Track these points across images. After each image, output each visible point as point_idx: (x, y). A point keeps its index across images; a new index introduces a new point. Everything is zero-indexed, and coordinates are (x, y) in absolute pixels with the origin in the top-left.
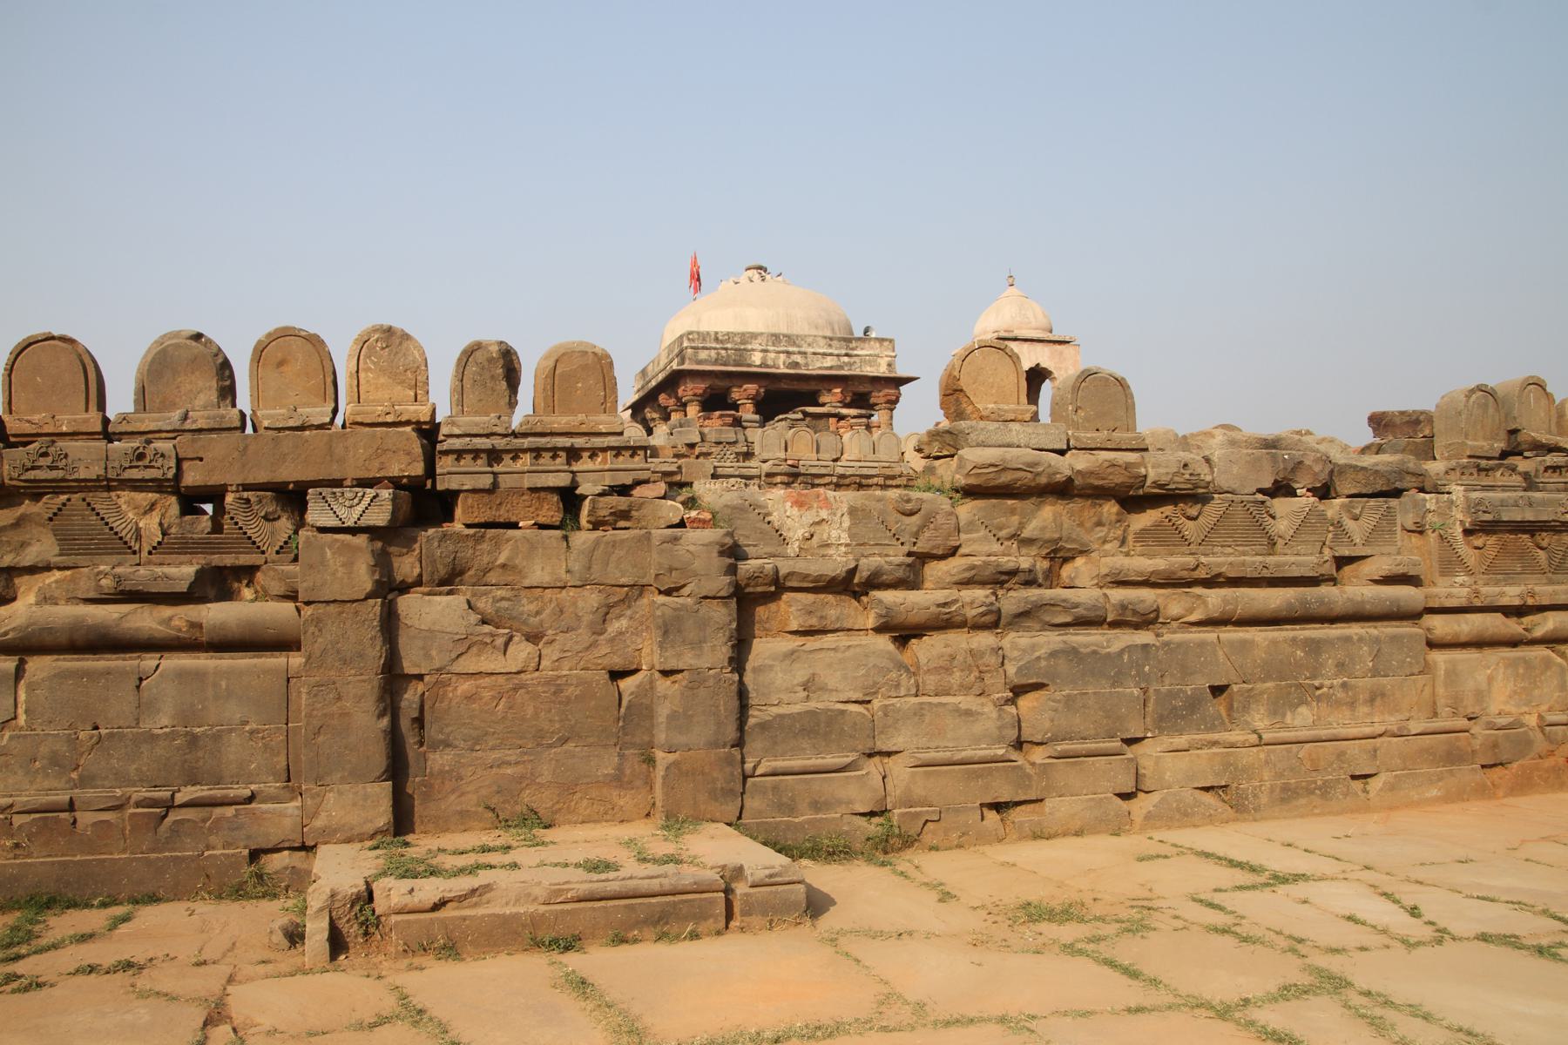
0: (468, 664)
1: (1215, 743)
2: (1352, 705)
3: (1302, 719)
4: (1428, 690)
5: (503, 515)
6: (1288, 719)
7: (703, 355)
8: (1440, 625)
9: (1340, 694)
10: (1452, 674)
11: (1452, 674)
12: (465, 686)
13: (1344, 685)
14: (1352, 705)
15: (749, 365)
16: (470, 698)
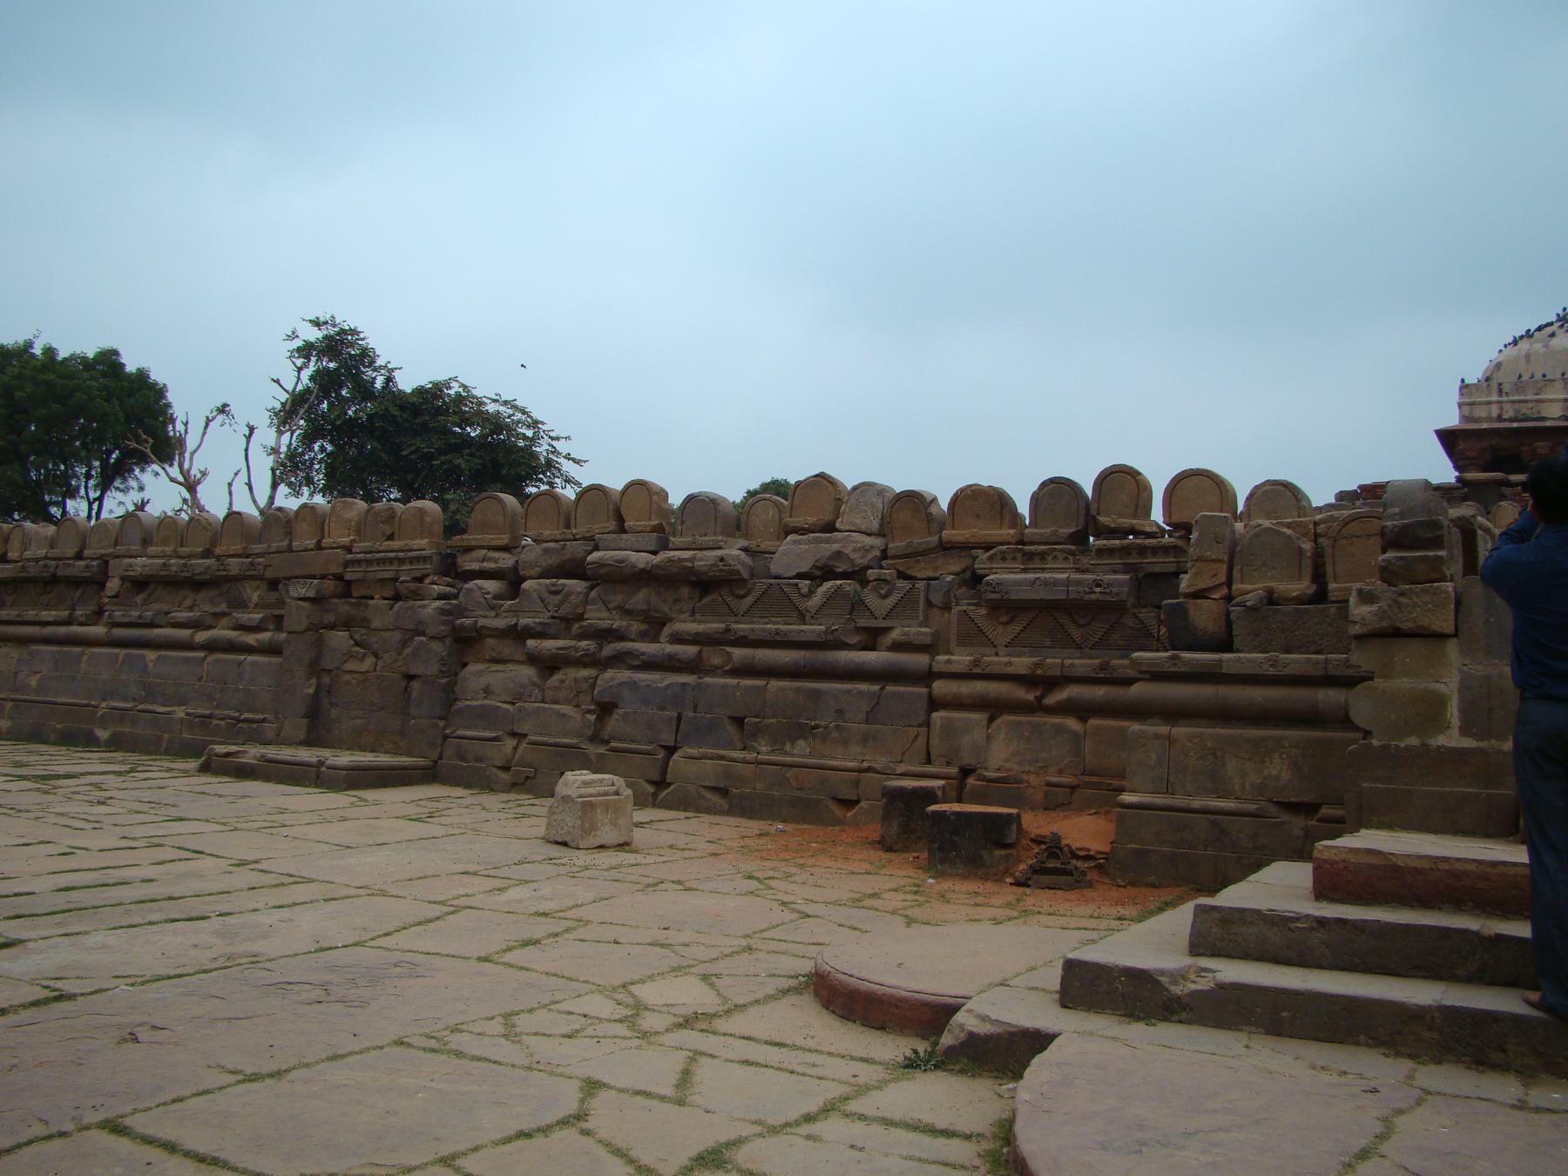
0: (350, 666)
1: (722, 758)
2: (846, 743)
3: (800, 750)
4: (921, 741)
5: (369, 593)
6: (788, 747)
7: (1480, 412)
8: (939, 687)
9: (835, 734)
10: (949, 730)
11: (949, 730)
12: (347, 677)
13: (837, 727)
14: (846, 743)
15: (1544, 419)
16: (348, 683)
